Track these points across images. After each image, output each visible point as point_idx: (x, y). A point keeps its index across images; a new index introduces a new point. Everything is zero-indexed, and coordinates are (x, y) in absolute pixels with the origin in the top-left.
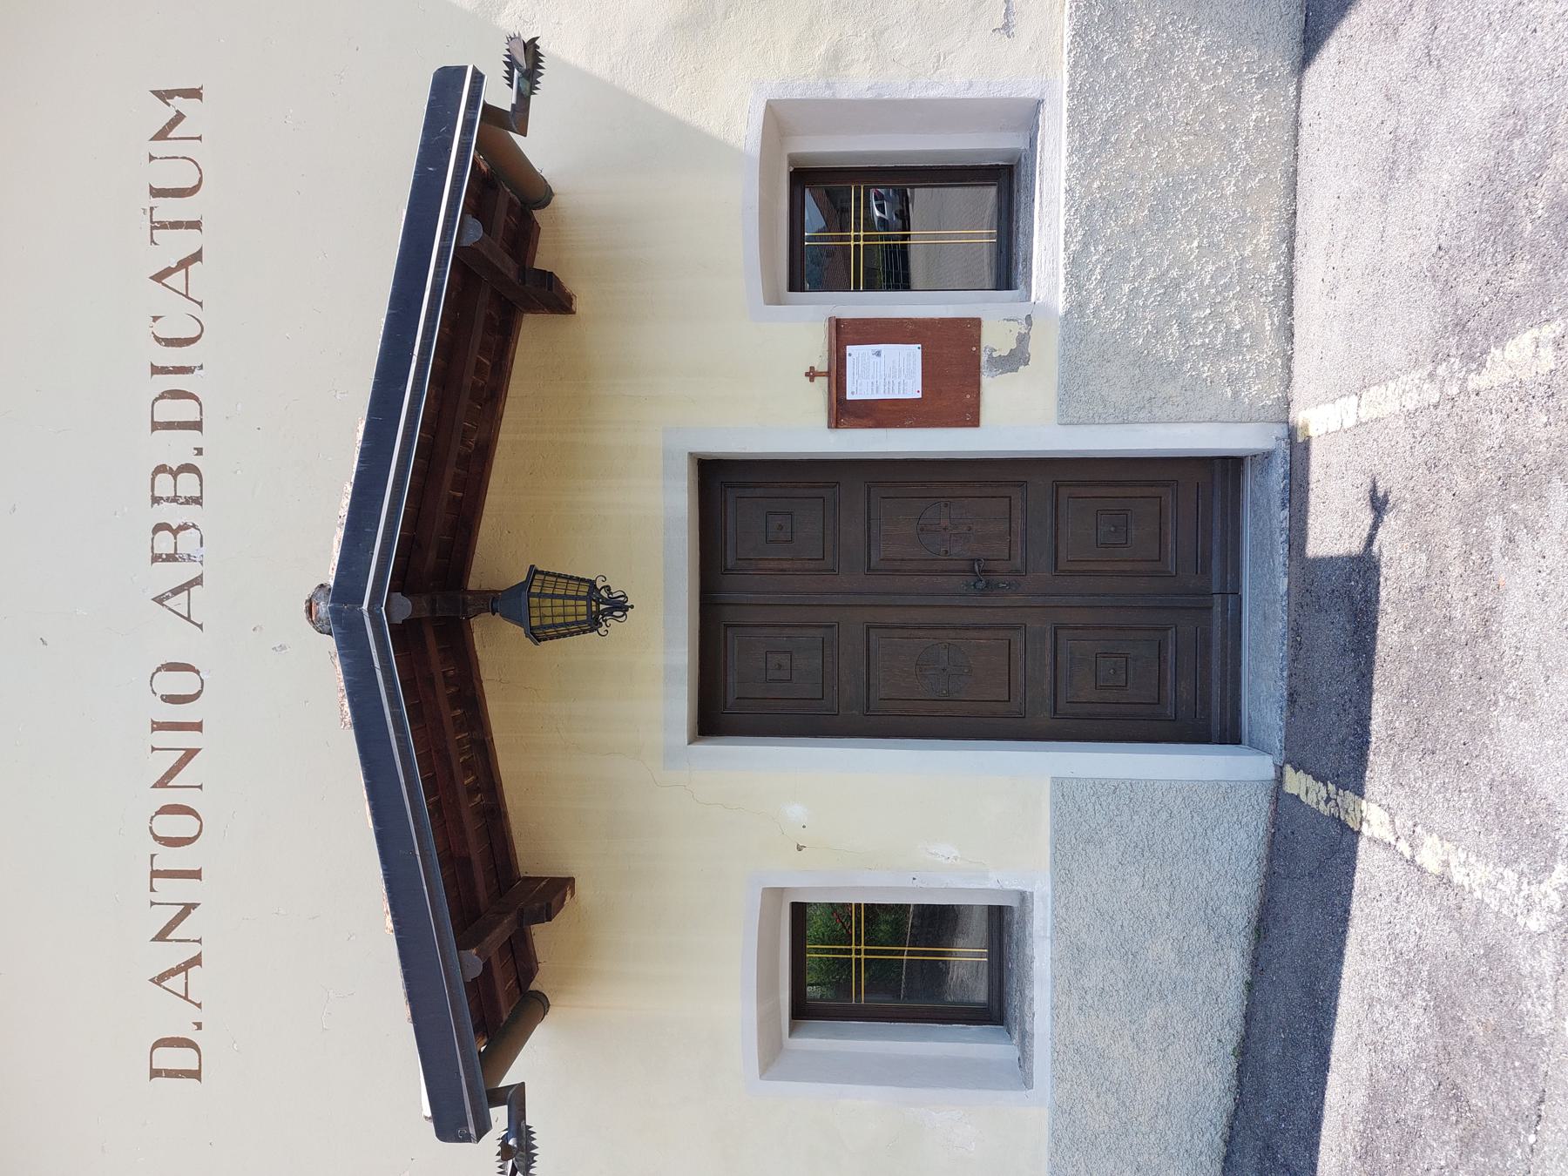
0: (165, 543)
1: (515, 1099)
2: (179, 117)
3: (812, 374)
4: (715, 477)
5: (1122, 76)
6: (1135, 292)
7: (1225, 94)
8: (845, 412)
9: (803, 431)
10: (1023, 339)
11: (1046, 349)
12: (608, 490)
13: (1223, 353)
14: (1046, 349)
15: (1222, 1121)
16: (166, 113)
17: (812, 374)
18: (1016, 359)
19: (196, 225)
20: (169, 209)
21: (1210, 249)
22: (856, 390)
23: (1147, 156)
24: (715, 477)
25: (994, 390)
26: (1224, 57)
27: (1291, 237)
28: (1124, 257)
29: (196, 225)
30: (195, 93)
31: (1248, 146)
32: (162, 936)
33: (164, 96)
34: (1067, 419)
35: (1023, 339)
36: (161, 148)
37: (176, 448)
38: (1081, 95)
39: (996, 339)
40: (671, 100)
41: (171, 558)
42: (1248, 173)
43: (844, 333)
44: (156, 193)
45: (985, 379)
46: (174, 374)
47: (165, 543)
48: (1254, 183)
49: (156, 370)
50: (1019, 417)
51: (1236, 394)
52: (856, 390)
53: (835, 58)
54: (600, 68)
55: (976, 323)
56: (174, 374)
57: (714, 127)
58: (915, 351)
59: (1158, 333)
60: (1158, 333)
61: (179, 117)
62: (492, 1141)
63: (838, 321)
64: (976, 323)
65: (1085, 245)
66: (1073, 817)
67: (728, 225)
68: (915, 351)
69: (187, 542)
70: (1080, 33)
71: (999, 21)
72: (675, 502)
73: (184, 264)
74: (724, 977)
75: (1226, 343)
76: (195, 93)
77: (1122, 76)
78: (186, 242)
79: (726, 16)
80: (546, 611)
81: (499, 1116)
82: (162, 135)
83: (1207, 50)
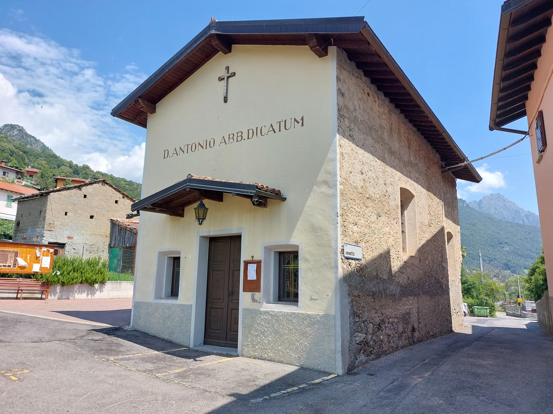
0: (231, 136)
1: (138, 214)
2: (298, 123)
3: (253, 257)
4: (237, 238)
5: (301, 325)
6: (263, 325)
7: (297, 348)
8: (247, 263)
9: (245, 256)
10: (256, 301)
11: (255, 306)
12: (222, 221)
13: (252, 344)
14: (255, 306)
15: (148, 332)
16: (299, 119)
17: (253, 257)
18: (254, 300)
19: (280, 131)
20: (283, 124)
21: (269, 342)
22: (250, 266)
23: (286, 330)
24: (237, 238)
25: (249, 295)
26: (304, 349)
27: (271, 360)
28: (269, 324)
29: (280, 131)
30: (302, 125)
31: (287, 353)
32: (181, 148)
33: (302, 119)
34: (244, 309)
35: (256, 301)
36: (293, 120)
37: (245, 136)
38: (297, 316)
39: (257, 295)
40: (300, 225)
41: (229, 138)
42: (283, 352)
43: (258, 263)
44: (285, 121)
45: (250, 293)
46: (258, 132)
47: (231, 136)
48: (281, 354)
49: (257, 128)
50: (245, 299)
51: (245, 346)
52: (250, 266)
53: (306, 260)
54: (305, 209)
55: (259, 291)
56: (258, 132)
57: (294, 234)
58: (255, 278)
59: (256, 330)
60: (256, 330)
61: (298, 123)
62: (131, 212)
63: (261, 262)
64: (259, 291)
65: (271, 315)
66: (186, 308)
67: (282, 239)
68: (255, 278)
69: (231, 140)
70: (309, 316)
71: (313, 297)
72: (233, 231)
73: (273, 130)
74: (170, 246)
75: (254, 344)
76: (302, 125)
77: (301, 325)
78: (277, 130)
79: (315, 235)
80: (201, 212)
81: (135, 212)
82: (295, 120)
83: (306, 345)
